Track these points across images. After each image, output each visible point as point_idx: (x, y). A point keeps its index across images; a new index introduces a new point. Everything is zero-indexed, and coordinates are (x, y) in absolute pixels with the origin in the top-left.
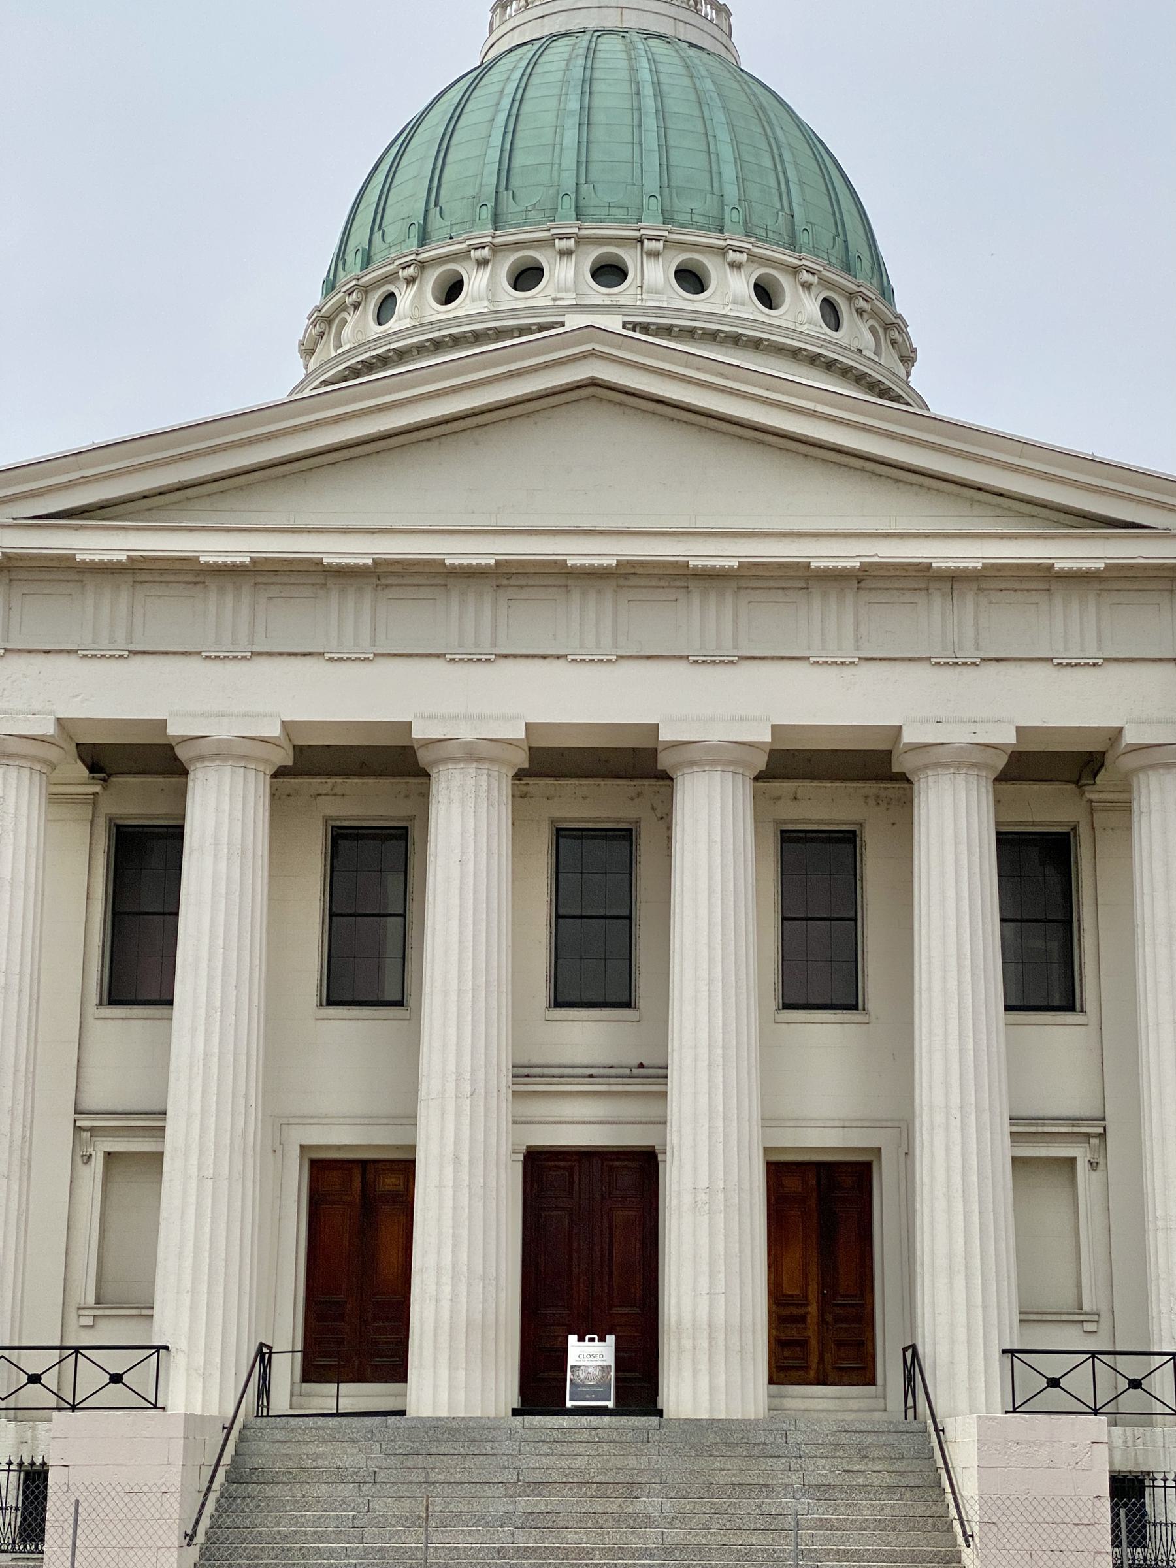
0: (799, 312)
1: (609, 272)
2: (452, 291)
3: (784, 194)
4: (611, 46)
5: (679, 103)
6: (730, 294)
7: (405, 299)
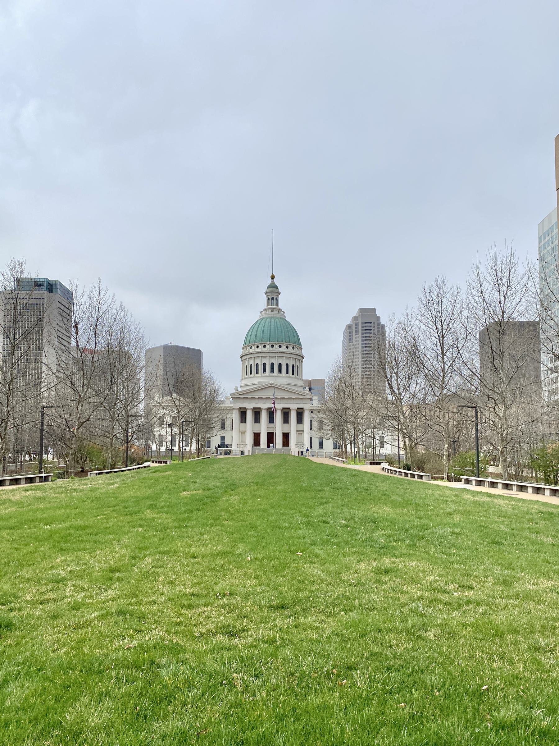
0: (290, 349)
1: (272, 346)
2: (258, 347)
3: (289, 336)
4: (273, 320)
5: (279, 328)
6: (284, 348)
7: (253, 347)
